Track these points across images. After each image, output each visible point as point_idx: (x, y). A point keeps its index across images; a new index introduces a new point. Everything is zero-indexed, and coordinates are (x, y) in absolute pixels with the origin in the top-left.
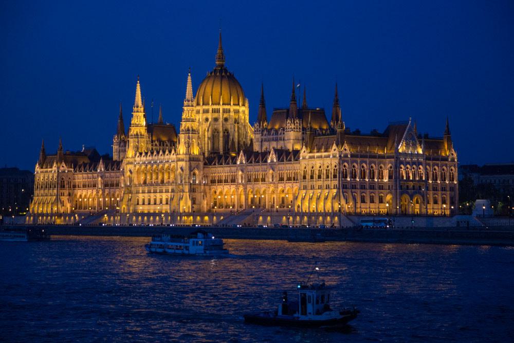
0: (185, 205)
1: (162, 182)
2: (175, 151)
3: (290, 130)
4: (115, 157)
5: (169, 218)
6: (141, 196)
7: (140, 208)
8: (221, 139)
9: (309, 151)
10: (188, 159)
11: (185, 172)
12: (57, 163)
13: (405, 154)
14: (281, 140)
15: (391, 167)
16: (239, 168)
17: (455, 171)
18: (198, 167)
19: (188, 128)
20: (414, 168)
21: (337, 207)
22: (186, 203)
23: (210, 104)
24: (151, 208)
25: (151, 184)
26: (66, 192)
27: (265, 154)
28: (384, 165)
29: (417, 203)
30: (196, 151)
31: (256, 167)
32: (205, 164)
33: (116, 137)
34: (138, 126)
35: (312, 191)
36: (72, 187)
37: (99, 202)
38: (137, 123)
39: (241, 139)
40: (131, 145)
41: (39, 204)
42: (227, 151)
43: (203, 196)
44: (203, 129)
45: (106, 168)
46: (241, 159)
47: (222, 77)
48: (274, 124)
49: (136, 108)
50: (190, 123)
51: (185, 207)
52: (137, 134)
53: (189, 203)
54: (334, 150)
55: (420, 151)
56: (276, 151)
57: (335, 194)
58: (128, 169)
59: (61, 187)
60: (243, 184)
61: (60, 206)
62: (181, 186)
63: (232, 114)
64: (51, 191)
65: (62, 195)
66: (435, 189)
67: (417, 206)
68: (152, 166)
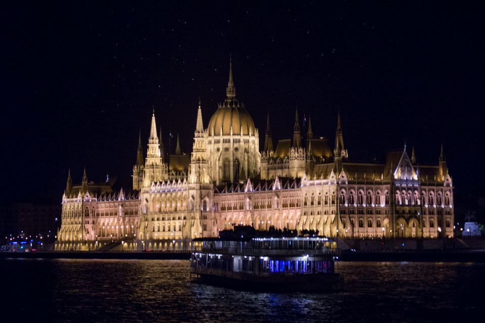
1: (176, 210)
2: (187, 179)
4: (135, 187)
5: (182, 244)
7: (156, 235)
8: (232, 168)
10: (198, 187)
12: (82, 193)
13: (400, 180)
14: (285, 168)
15: (387, 193)
16: (246, 195)
17: (450, 196)
18: (208, 195)
19: (199, 158)
20: (409, 194)
21: (335, 231)
22: (197, 230)
23: (221, 134)
24: (167, 235)
25: (166, 213)
26: (91, 220)
27: (270, 182)
28: (381, 191)
29: (414, 226)
30: (206, 180)
32: (215, 192)
33: (136, 167)
35: (312, 217)
36: (96, 215)
37: (120, 229)
38: (152, 154)
39: (251, 168)
40: (147, 174)
41: (66, 231)
42: (237, 178)
43: (214, 223)
44: (215, 159)
45: (126, 197)
46: (249, 187)
50: (201, 153)
51: (196, 234)
52: (153, 165)
53: (200, 229)
54: (332, 177)
55: (415, 177)
56: (280, 178)
57: (333, 220)
58: (144, 198)
59: (86, 215)
60: (251, 211)
61: (84, 234)
64: (76, 220)
65: (86, 223)
66: (431, 213)
67: (414, 229)
68: (166, 194)
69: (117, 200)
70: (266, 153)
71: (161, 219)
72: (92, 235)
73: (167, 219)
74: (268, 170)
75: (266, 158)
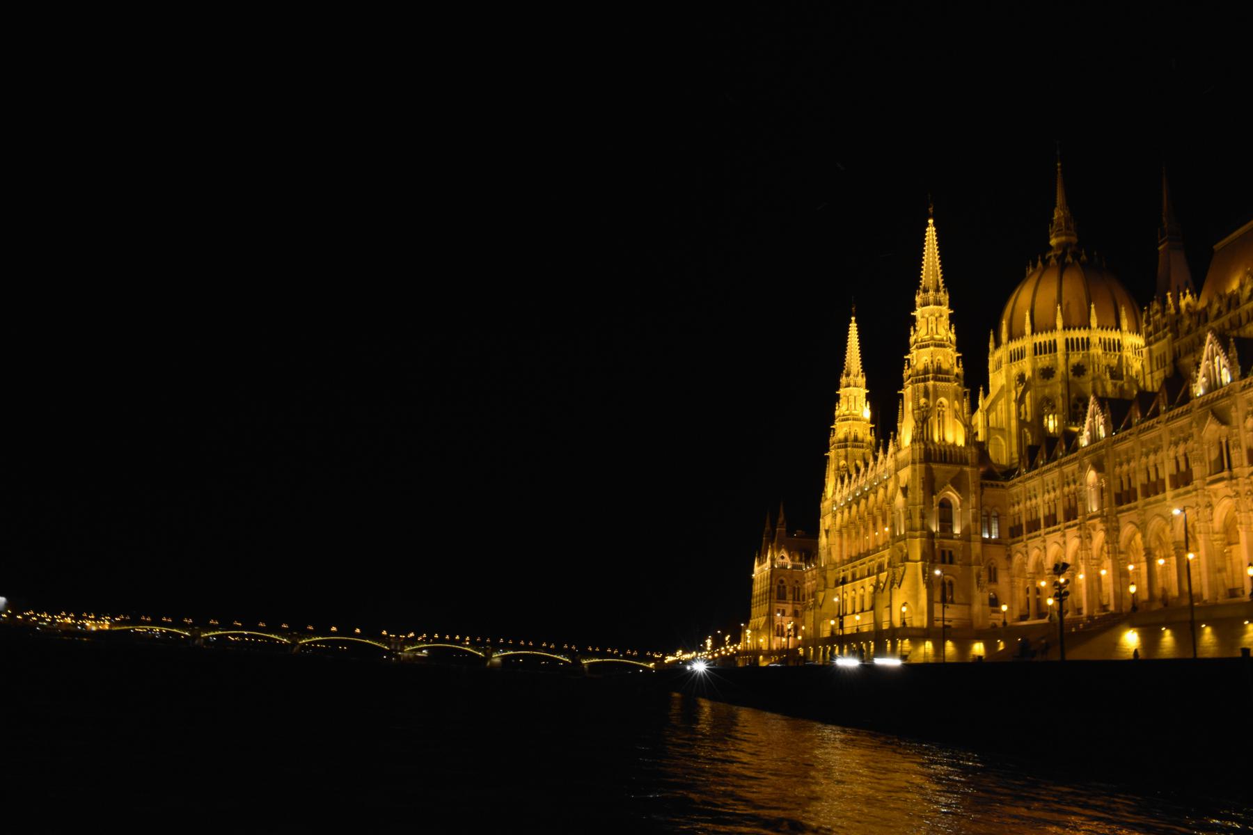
16: (1086, 460)
18: (958, 484)
22: (915, 597)
23: (1028, 329)
27: (1177, 384)
30: (954, 435)
31: (1145, 437)
46: (1093, 427)
47: (1063, 267)
52: (846, 440)
62: (902, 543)
63: (1097, 351)
70: (1164, 302)
71: (850, 578)
74: (1175, 360)
75: (1164, 321)
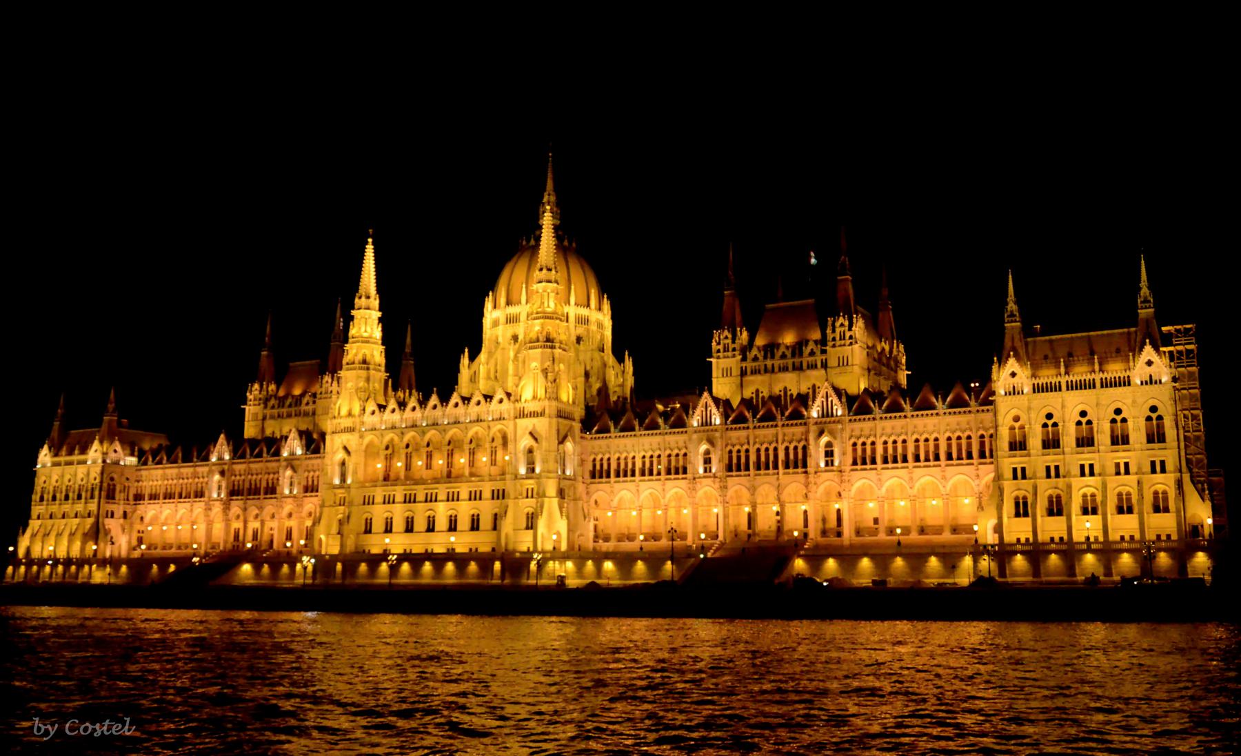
0: (553, 530)
3: (848, 342)
4: (250, 431)
5: (497, 565)
6: (379, 513)
7: (376, 544)
9: (1028, 372)
10: (554, 412)
11: (544, 444)
12: (101, 442)
14: (812, 366)
19: (548, 334)
33: (256, 386)
34: (368, 342)
36: (131, 497)
38: (365, 335)
45: (237, 454)
48: (776, 330)
49: (363, 299)
52: (364, 362)
53: (562, 525)
63: (593, 328)
68: (424, 433)
69: (207, 459)
72: (121, 543)
73: (421, 497)
74: (743, 373)
